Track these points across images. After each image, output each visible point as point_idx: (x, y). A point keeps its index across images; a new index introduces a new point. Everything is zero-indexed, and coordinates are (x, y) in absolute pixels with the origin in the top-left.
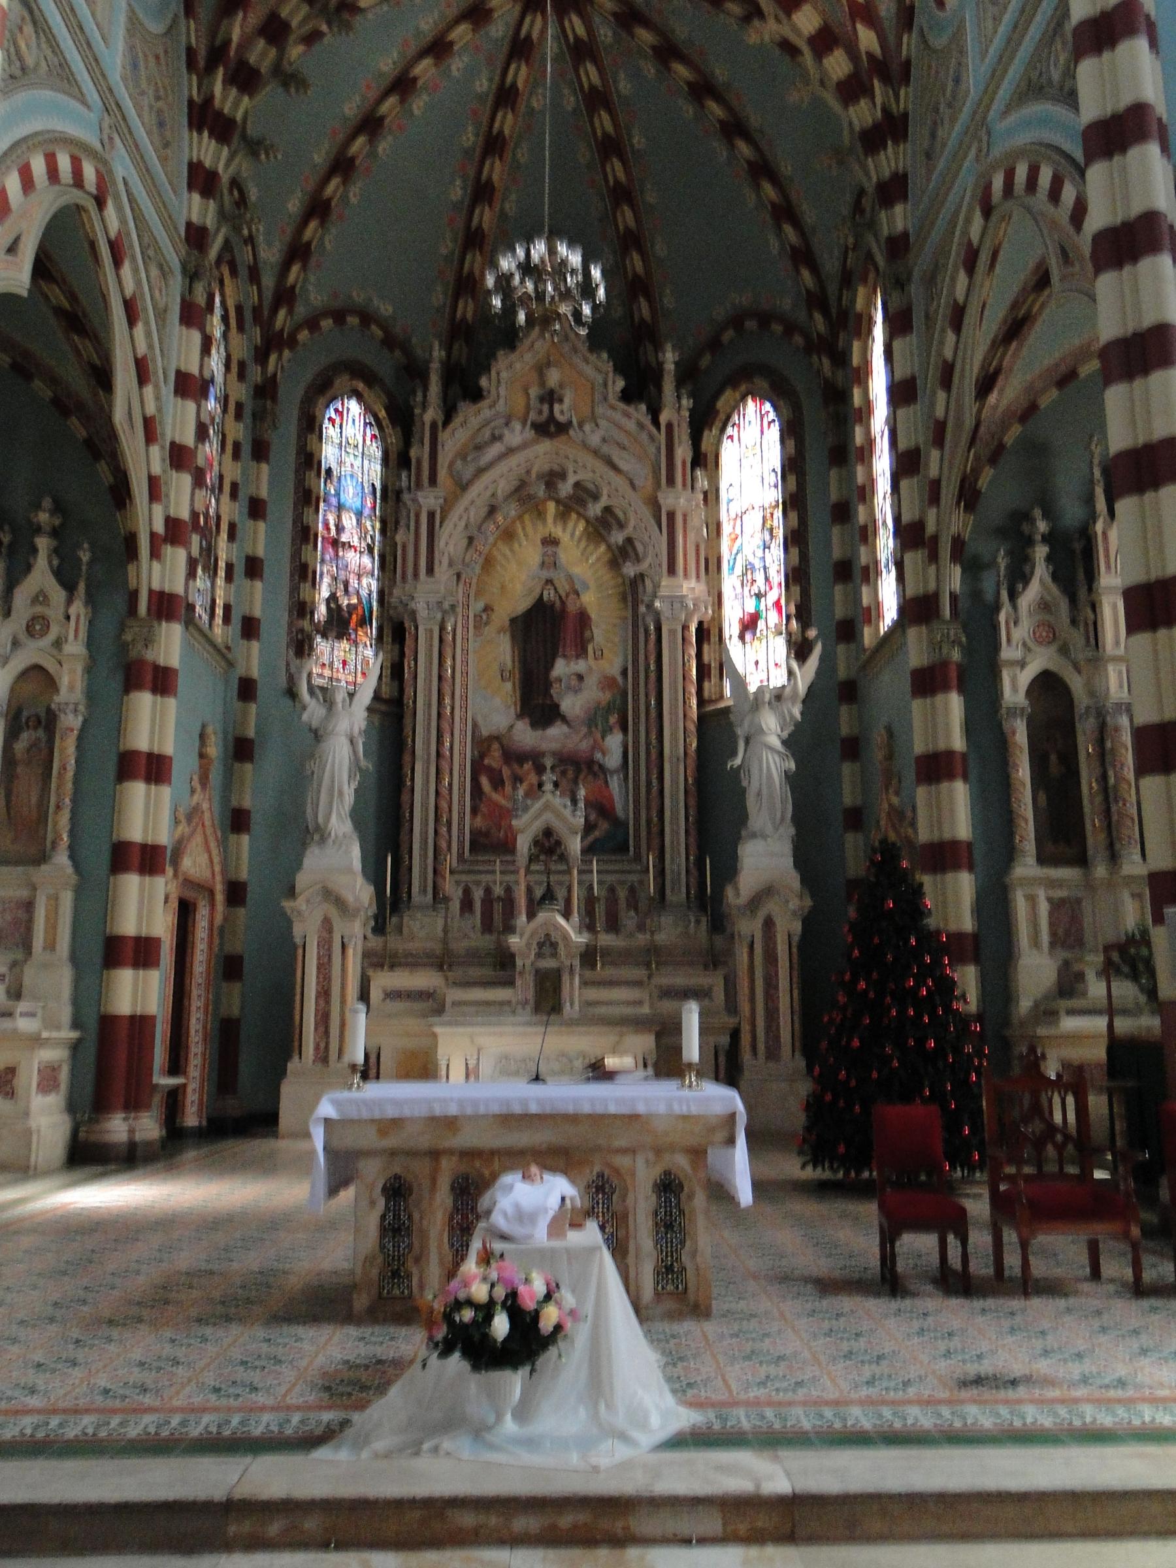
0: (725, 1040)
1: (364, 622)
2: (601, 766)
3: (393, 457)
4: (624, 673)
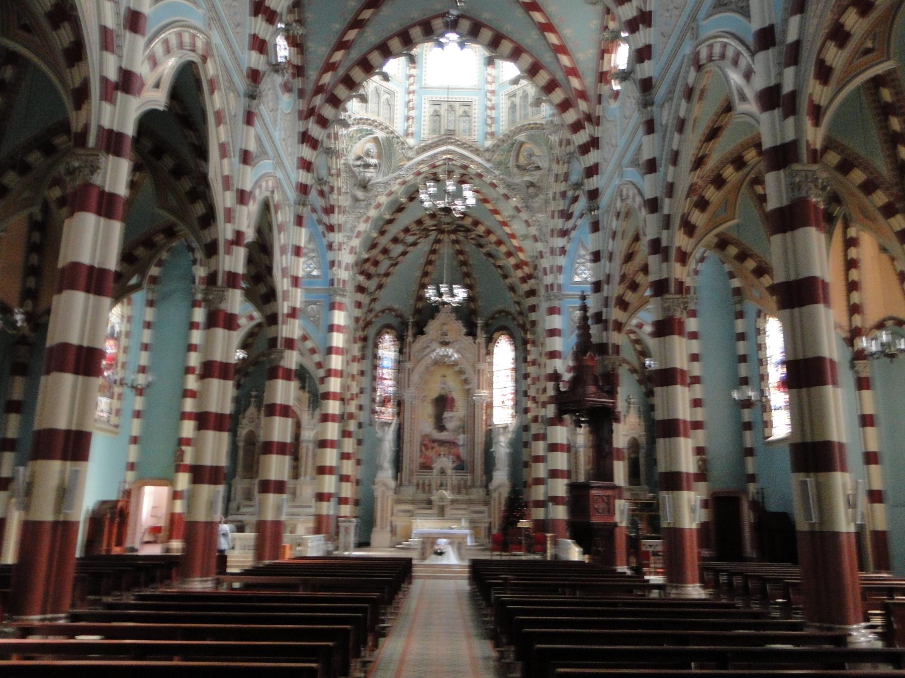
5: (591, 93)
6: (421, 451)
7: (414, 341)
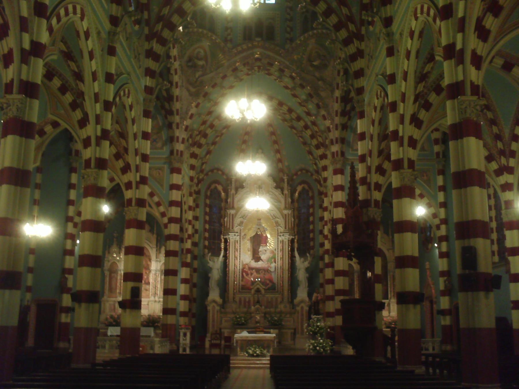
4: (275, 250)
5: (357, 18)
6: (242, 275)
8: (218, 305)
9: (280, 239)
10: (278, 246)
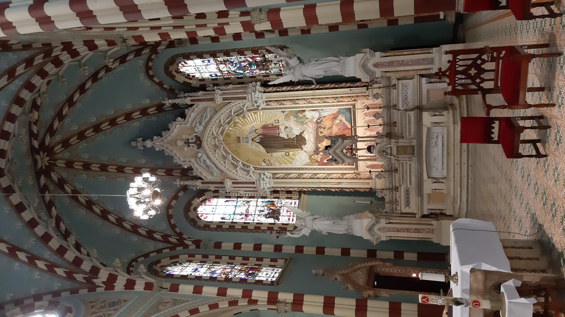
0: (424, 80)
1: (272, 203)
2: (319, 119)
3: (215, 194)
4: (283, 112)
7: (201, 179)
8: (377, 222)
9: (263, 106)
10: (277, 108)
